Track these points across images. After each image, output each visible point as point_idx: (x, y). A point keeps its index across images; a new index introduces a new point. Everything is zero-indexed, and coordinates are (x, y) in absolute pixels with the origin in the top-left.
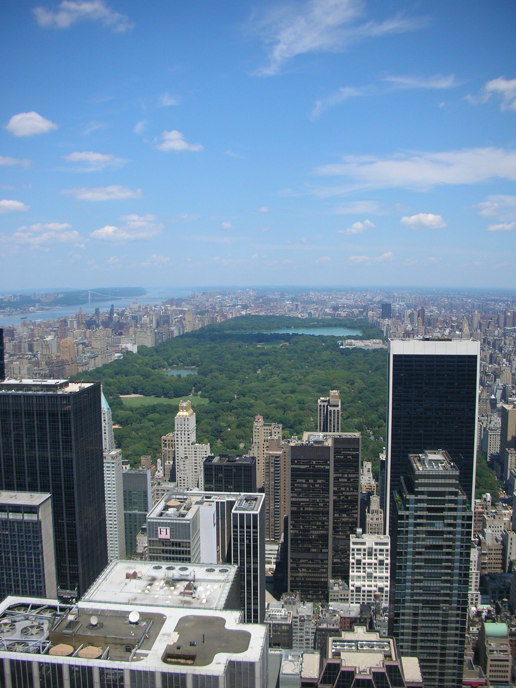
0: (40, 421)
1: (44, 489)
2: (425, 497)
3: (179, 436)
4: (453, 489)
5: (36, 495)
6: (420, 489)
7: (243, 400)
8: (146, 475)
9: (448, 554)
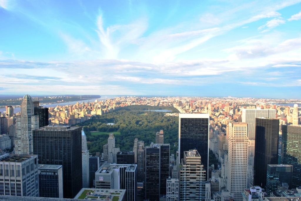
1: (60, 163)
2: (189, 166)
4: (199, 163)
5: (58, 165)
6: (188, 163)
7: (132, 133)
8: (97, 159)
9: (198, 185)
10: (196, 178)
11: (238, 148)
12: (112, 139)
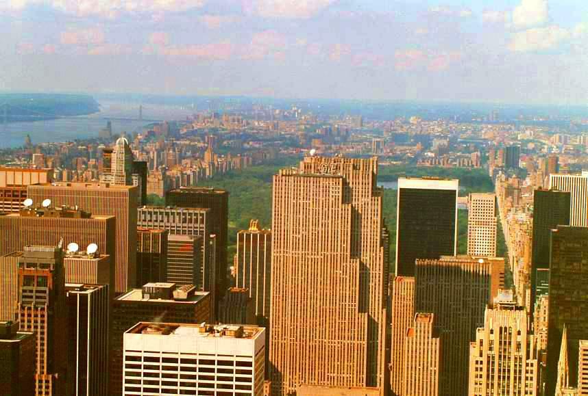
11: (479, 235)
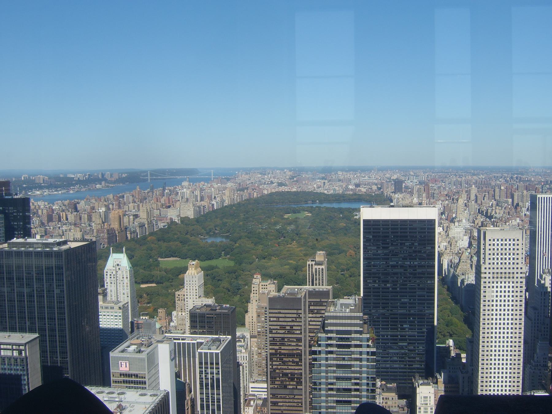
0: (30, 273)
1: (32, 330)
2: (334, 335)
3: (188, 291)
4: (358, 329)
6: (329, 328)
9: (357, 384)
10: (350, 365)
11: (499, 294)
12: (196, 274)
